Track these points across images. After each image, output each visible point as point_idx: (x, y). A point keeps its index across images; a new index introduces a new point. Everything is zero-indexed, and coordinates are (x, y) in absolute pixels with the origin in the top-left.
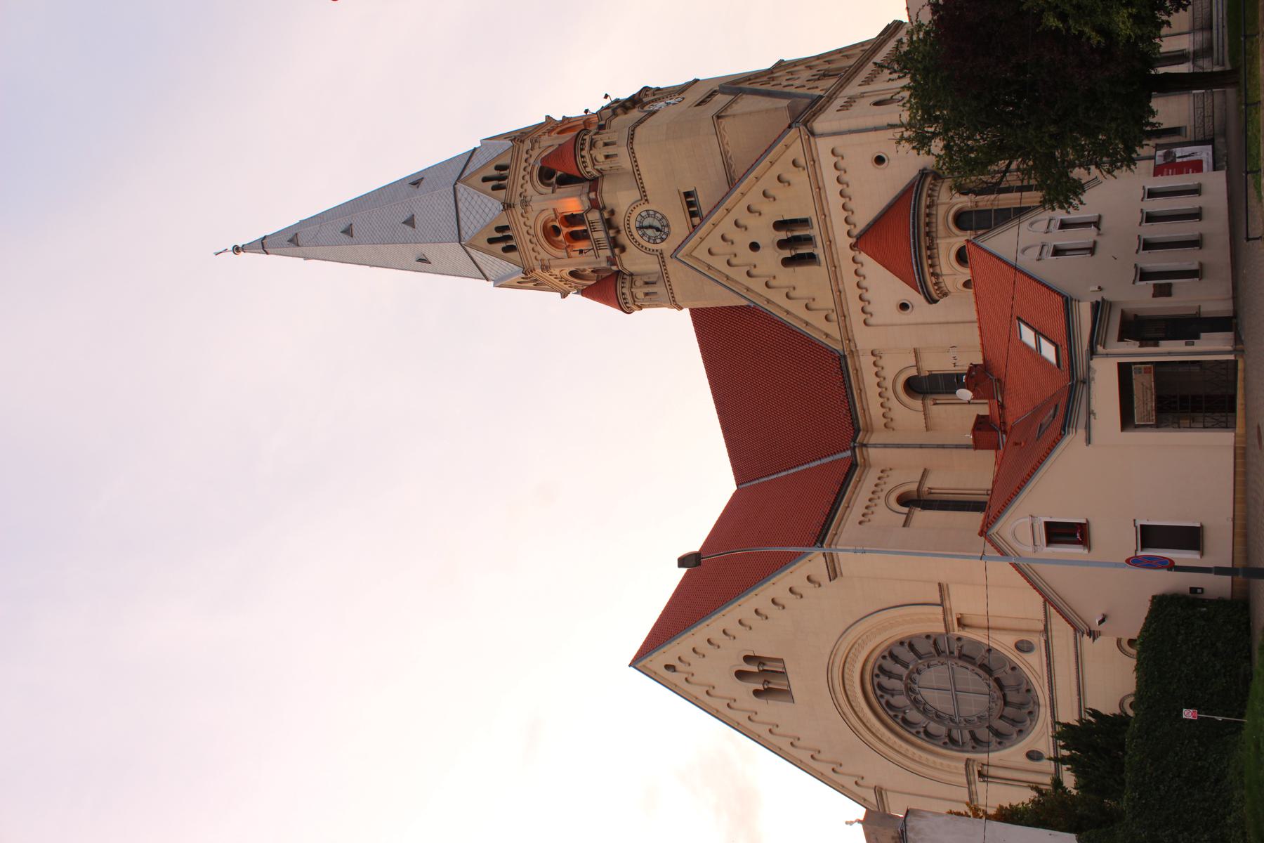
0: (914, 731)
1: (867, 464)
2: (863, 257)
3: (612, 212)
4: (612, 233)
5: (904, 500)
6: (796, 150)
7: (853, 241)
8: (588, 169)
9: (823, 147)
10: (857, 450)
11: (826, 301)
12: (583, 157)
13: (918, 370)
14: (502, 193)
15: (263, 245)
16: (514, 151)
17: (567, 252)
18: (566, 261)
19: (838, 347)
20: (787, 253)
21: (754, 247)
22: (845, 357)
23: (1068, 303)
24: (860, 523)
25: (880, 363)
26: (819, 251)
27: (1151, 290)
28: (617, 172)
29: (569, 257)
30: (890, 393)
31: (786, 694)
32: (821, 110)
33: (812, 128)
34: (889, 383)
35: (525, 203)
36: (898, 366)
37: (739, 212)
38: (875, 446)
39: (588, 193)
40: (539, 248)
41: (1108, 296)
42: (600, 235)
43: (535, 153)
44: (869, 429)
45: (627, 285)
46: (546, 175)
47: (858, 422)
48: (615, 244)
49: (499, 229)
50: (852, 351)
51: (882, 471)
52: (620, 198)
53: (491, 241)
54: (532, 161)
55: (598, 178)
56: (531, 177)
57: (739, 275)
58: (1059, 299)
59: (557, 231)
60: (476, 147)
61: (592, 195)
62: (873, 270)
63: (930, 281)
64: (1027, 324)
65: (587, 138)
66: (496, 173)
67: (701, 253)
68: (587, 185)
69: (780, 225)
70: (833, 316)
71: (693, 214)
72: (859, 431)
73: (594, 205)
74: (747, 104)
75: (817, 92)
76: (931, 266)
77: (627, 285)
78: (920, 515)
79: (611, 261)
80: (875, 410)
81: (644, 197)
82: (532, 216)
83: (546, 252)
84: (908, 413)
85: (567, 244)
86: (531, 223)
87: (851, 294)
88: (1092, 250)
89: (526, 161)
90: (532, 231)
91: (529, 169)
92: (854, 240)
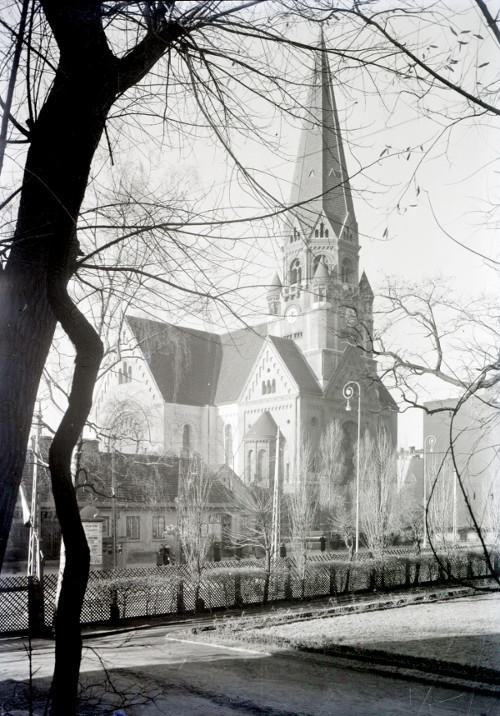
21: (269, 370)
26: (267, 396)
62: (259, 414)
69: (274, 381)
83: (290, 259)
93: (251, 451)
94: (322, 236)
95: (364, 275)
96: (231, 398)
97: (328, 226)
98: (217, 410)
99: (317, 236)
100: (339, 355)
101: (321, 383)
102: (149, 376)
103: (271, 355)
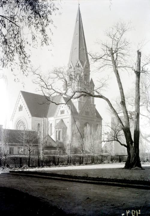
15: (79, 11)
21: (62, 107)
26: (62, 115)
31: (19, 111)
69: (64, 110)
93: (57, 131)
94: (79, 67)
95: (92, 79)
96: (51, 116)
97: (80, 64)
98: (48, 119)
99: (77, 67)
100: (84, 103)
101: (78, 111)
102: (27, 109)
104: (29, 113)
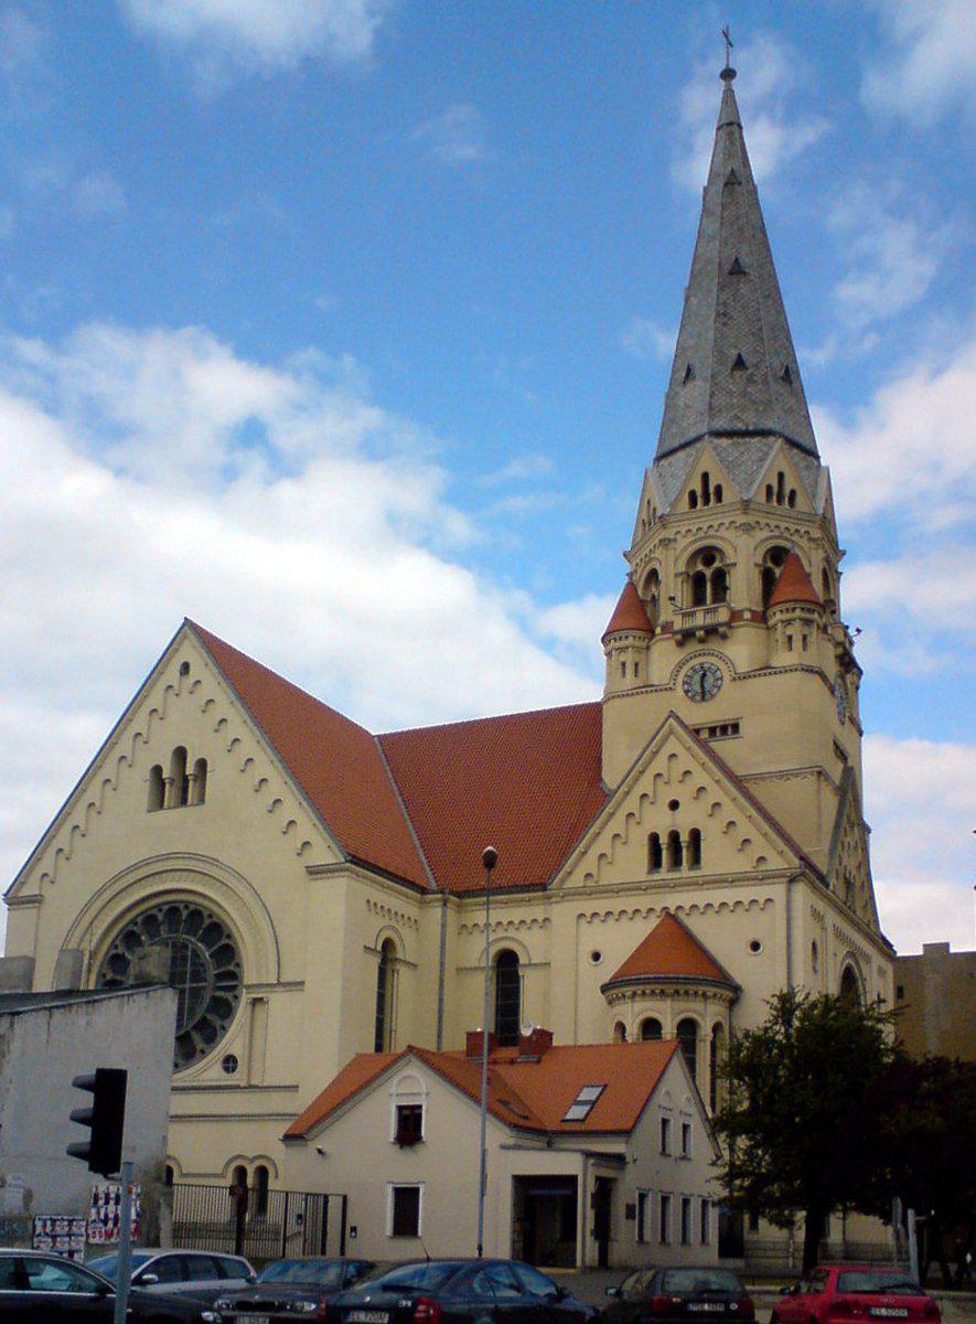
0: (118, 942)
1: (422, 903)
2: (653, 922)
3: (724, 637)
4: (700, 634)
5: (388, 945)
6: (776, 863)
7: (672, 911)
8: (778, 614)
9: (777, 891)
10: (440, 896)
11: (610, 876)
12: (794, 609)
13: (525, 966)
14: (762, 498)
16: (810, 518)
17: (681, 574)
18: (673, 568)
19: (554, 885)
20: (664, 840)
21: (674, 805)
22: (546, 890)
23: (626, 1133)
24: (368, 901)
25: (536, 928)
26: (663, 874)
27: (631, 1203)
28: (770, 649)
29: (676, 575)
30: (501, 934)
32: (815, 888)
33: (799, 881)
34: (512, 933)
35: (748, 528)
36: (530, 946)
37: (715, 795)
38: (444, 915)
39: (750, 610)
40: (691, 539)
41: (630, 1167)
42: (700, 619)
43: (804, 543)
44: (460, 908)
45: (637, 643)
46: (777, 555)
47: (469, 897)
48: (687, 636)
49: (719, 490)
50: (551, 897)
51: (416, 921)
52: (741, 649)
53: (705, 477)
54: (795, 538)
55: (766, 623)
56: (777, 537)
57: (645, 785)
58: (630, 1124)
59: (709, 561)
60: (822, 460)
61: (747, 615)
62: (641, 930)
63: (628, 991)
64: (601, 1094)
65: (816, 616)
66: (787, 491)
67: (672, 746)
68: (759, 608)
69: (696, 836)
70: (590, 883)
71: (712, 731)
72: (459, 897)
73: (735, 615)
74: (830, 801)
75: (832, 881)
76: (644, 993)
77: (637, 643)
78: (375, 961)
79: (667, 627)
80: (479, 917)
81: (740, 678)
82: (730, 535)
83: (685, 546)
84: (478, 951)
85: (691, 574)
86: (723, 533)
87: (616, 904)
88: (664, 1152)
89: (797, 531)
90: (712, 532)
91: (786, 534)
92: (673, 913)
103: (685, 761)
104: (309, 828)
